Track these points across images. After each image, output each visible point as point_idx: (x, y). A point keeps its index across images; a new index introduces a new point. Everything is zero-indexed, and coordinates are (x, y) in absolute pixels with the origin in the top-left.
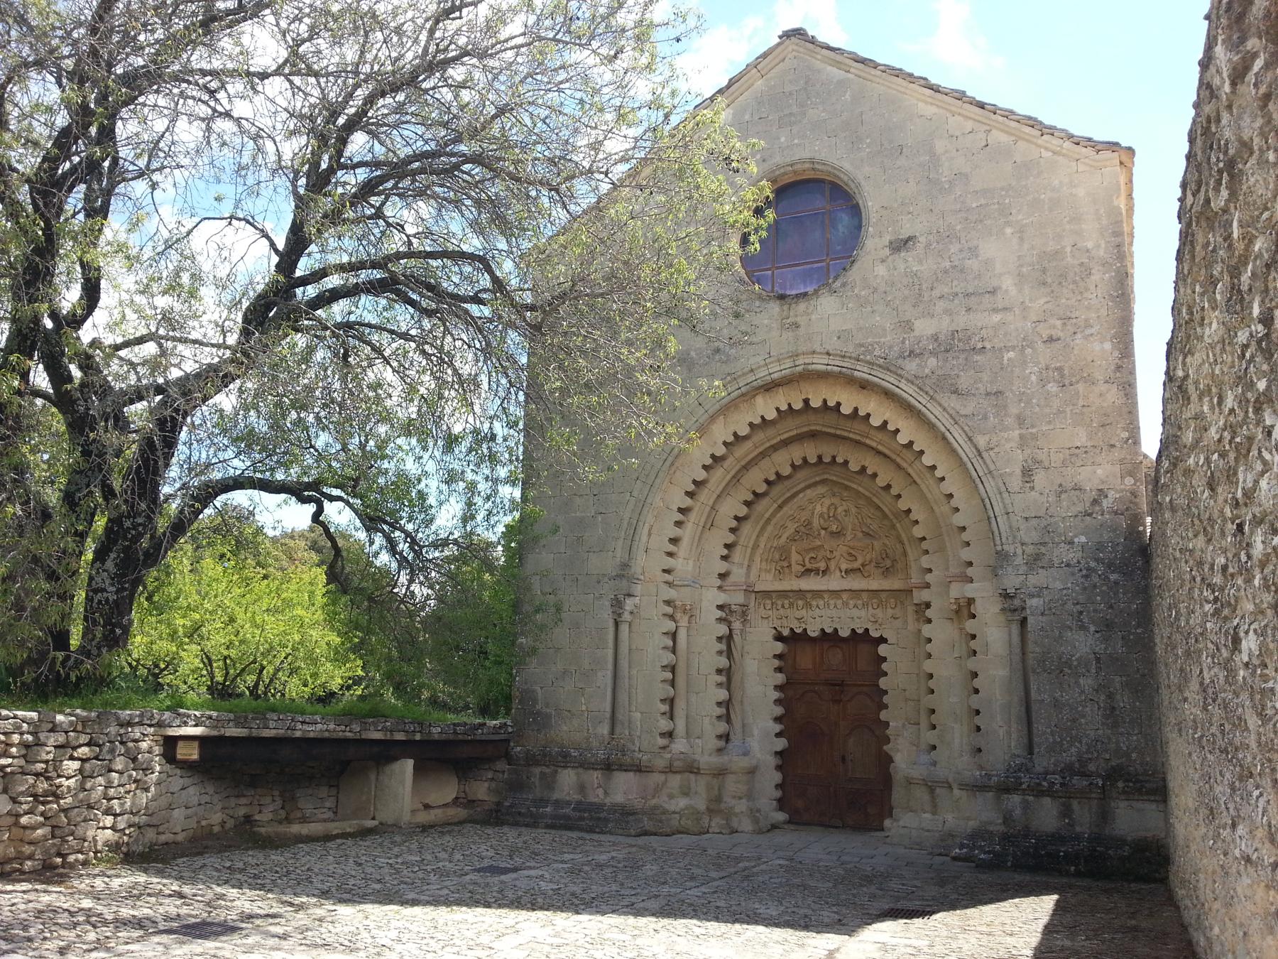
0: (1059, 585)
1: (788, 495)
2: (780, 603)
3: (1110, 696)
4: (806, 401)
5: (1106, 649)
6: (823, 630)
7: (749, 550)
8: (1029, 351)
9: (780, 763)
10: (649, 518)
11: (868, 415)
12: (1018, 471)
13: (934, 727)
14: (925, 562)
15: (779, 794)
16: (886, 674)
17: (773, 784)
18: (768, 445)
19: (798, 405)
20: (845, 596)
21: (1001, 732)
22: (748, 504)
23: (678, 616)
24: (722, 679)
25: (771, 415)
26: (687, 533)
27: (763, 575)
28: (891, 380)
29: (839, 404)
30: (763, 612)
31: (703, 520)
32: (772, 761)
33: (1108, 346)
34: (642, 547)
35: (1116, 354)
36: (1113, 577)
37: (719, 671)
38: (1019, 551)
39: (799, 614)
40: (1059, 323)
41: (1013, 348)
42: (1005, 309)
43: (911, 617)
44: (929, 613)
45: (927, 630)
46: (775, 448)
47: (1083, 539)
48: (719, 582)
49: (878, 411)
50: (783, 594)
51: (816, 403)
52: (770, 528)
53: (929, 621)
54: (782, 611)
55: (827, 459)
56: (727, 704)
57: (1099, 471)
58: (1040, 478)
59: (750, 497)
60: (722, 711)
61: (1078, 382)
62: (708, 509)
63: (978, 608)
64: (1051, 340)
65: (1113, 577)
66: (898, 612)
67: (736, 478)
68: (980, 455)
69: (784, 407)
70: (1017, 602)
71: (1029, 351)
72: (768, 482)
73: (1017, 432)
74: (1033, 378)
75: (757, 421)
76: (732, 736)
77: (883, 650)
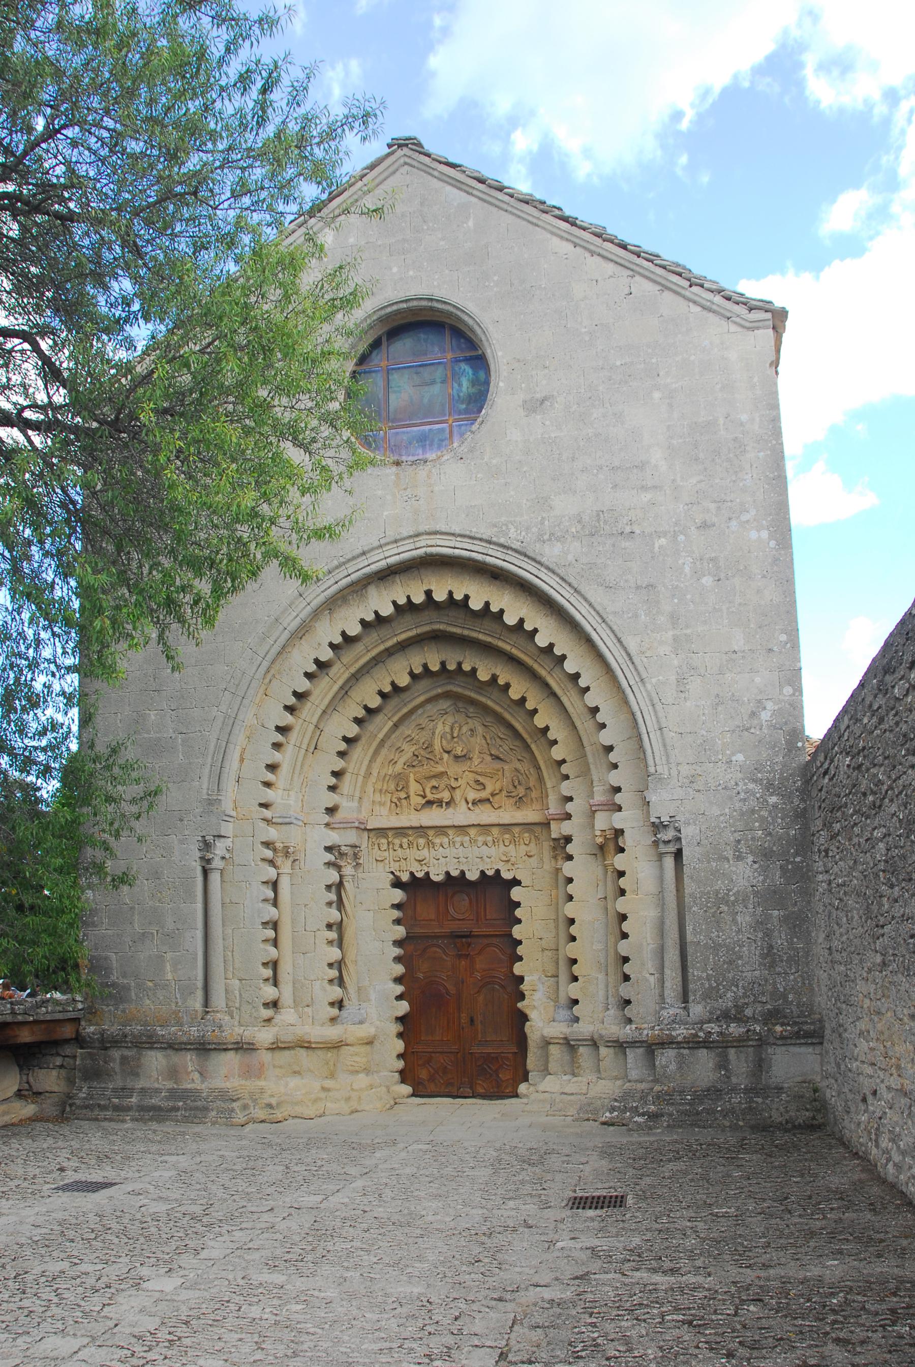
0: (716, 811)
1: (405, 710)
2: (397, 842)
3: (768, 934)
4: (428, 593)
5: (764, 881)
6: (448, 873)
7: (360, 779)
8: (681, 538)
9: (401, 1029)
10: (240, 739)
11: (502, 611)
12: (673, 678)
13: (575, 979)
14: (566, 788)
15: (401, 1064)
17: (395, 1054)
18: (382, 647)
19: (419, 598)
21: (652, 979)
22: (358, 721)
24: (333, 935)
25: (387, 610)
26: (284, 758)
28: (529, 568)
29: (467, 597)
30: (377, 853)
31: (306, 741)
33: (765, 534)
34: (233, 777)
35: (773, 543)
36: (773, 799)
37: (329, 926)
38: (674, 772)
40: (713, 506)
41: (665, 534)
42: (655, 487)
43: (547, 854)
44: (570, 849)
45: (568, 869)
46: (389, 653)
47: (740, 757)
49: (513, 607)
50: (401, 831)
51: (440, 596)
52: (384, 751)
53: (570, 858)
55: (452, 667)
56: (339, 965)
57: (758, 680)
58: (695, 685)
59: (361, 713)
60: (334, 973)
61: (734, 576)
62: (312, 727)
63: (628, 841)
64: (705, 526)
65: (773, 799)
67: (345, 691)
68: (631, 659)
69: (402, 601)
70: (669, 834)
71: (681, 538)
72: (382, 694)
73: (671, 633)
74: (687, 569)
75: (370, 617)
76: (346, 1003)
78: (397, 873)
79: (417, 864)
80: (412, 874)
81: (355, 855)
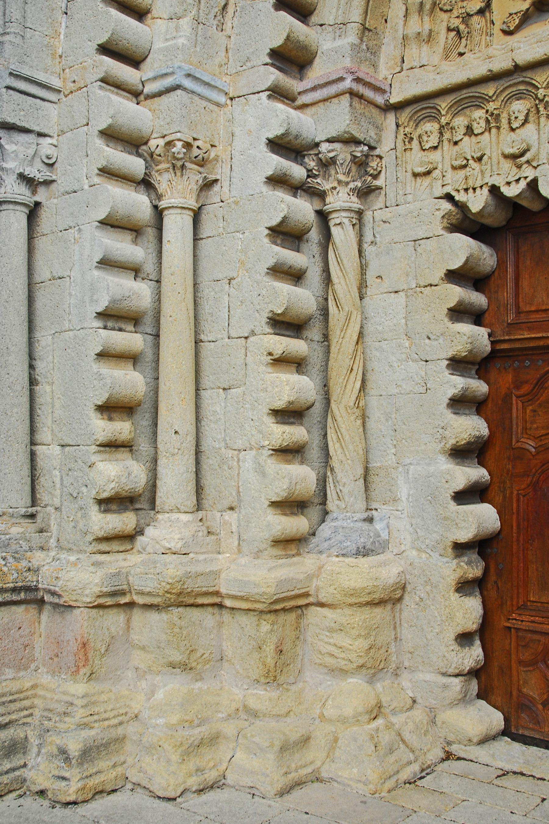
2: (460, 122)
23: (163, 181)
27: (417, 54)
30: (416, 159)
32: (453, 569)
48: (273, 76)
50: (466, 93)
54: (468, 146)
78: (460, 197)
79: (507, 165)
80: (494, 190)
81: (361, 164)
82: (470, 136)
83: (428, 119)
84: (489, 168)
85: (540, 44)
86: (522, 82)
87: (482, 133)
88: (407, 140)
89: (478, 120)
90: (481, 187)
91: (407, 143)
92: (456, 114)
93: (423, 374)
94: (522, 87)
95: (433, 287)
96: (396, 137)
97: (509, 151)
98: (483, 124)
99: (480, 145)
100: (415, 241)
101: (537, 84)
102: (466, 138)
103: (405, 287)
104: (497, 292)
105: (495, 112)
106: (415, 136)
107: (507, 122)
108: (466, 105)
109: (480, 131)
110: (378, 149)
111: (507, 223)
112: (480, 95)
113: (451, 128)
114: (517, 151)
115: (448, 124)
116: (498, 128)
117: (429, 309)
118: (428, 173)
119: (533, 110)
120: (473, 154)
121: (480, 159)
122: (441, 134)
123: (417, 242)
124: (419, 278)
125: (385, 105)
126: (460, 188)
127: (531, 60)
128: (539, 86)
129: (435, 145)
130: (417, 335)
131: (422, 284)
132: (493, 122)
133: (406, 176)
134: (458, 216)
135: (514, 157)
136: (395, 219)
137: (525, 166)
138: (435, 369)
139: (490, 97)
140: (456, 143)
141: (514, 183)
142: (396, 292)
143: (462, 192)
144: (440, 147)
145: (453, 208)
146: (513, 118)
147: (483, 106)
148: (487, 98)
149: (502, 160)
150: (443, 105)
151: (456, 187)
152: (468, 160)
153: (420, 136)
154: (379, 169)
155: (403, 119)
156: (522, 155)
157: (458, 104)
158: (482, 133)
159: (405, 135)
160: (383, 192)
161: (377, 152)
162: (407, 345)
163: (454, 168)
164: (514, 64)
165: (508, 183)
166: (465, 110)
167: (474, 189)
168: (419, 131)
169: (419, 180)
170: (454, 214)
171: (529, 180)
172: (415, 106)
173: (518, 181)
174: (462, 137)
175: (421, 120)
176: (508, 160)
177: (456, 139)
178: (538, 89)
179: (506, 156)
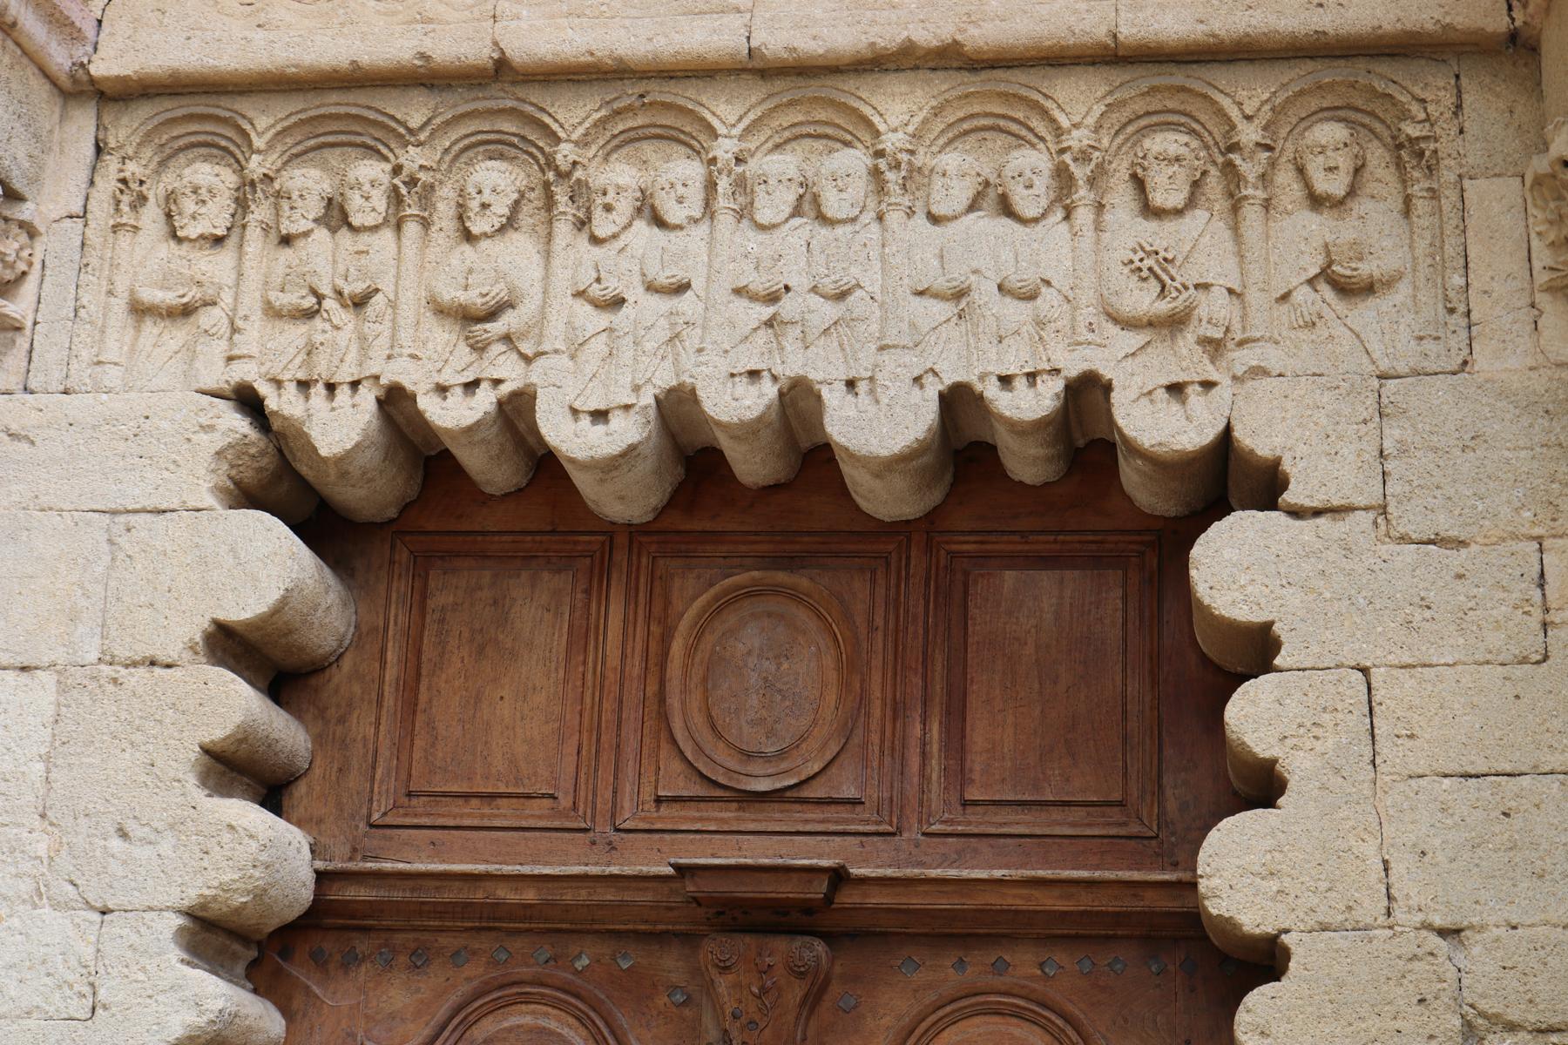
2: (309, 182)
16: (1262, 786)
20: (897, 109)
39: (465, 274)
54: (323, 255)
66: (1376, 233)
77: (1232, 567)
79: (443, 336)
80: (395, 402)
82: (333, 231)
83: (203, 151)
84: (387, 333)
85: (577, 21)
86: (512, 112)
87: (375, 229)
88: (126, 199)
89: (367, 187)
90: (355, 385)
91: (125, 208)
92: (297, 156)
93: (88, 952)
94: (508, 126)
95: (157, 670)
96: (92, 183)
97: (451, 294)
98: (380, 202)
99: (364, 260)
100: (114, 513)
101: (555, 126)
102: (322, 234)
103: (60, 656)
104: (342, 720)
105: (423, 176)
106: (155, 192)
107: (452, 212)
108: (331, 139)
109: (370, 220)
110: (29, 205)
111: (401, 512)
112: (381, 118)
113: (278, 195)
114: (479, 301)
115: (268, 179)
116: (426, 224)
117: (138, 737)
118: (187, 311)
119: (532, 195)
120: (340, 283)
121: (359, 303)
122: (242, 204)
123: (122, 519)
124: (113, 633)
125: (72, 77)
126: (286, 376)
127: (549, 57)
128: (562, 134)
129: (220, 232)
130: (82, 820)
131: (122, 653)
132: (407, 201)
133: (107, 308)
134: (264, 462)
135: (468, 317)
136: (52, 432)
137: (499, 348)
138: (134, 938)
139: (410, 131)
140: (286, 240)
141: (459, 391)
142: (23, 669)
143: (291, 388)
144: (232, 242)
145: (253, 434)
146: (474, 205)
147: (385, 151)
148: (402, 130)
149: (429, 319)
150: (262, 122)
151: (276, 371)
152: (320, 298)
153: (171, 197)
154: (22, 267)
155: (122, 134)
156: (492, 315)
157: (307, 128)
158: (375, 229)
159: (124, 181)
160: (22, 343)
161: (26, 212)
162: (42, 849)
163: (273, 313)
164: (496, 56)
165: (442, 390)
166: (326, 152)
167: (331, 388)
168: (169, 180)
169: (150, 328)
170: (253, 451)
171: (505, 389)
172: (168, 103)
173: (471, 386)
174: (311, 225)
175: (181, 149)
176: (448, 323)
177: (287, 227)
178: (558, 140)
179: (442, 311)
